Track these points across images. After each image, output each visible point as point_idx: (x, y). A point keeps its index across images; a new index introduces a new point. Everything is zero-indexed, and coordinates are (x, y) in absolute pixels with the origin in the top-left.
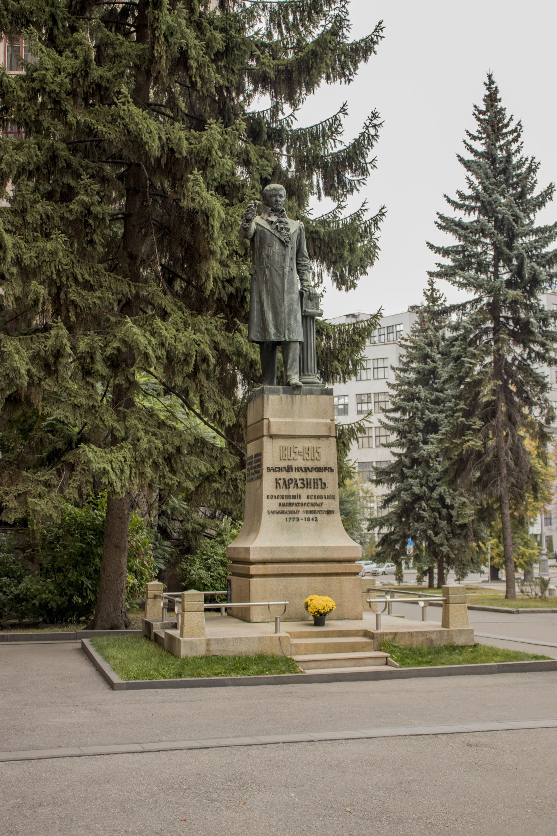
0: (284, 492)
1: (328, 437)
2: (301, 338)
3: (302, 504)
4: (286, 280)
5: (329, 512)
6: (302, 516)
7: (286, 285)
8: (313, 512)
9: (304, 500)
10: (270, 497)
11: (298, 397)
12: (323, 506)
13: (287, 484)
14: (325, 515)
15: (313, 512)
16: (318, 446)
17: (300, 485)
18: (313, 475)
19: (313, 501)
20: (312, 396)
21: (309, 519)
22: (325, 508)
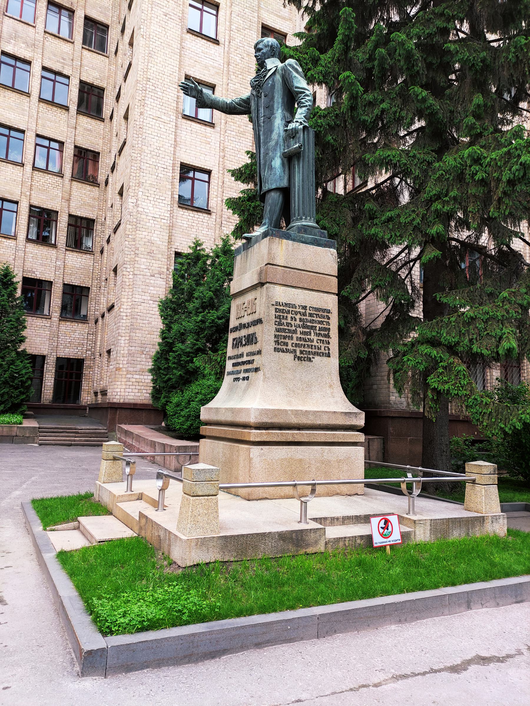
0: (236, 352)
1: (261, 284)
2: (284, 183)
3: (243, 363)
4: (261, 133)
5: (257, 370)
6: (242, 375)
7: (262, 137)
8: (246, 371)
9: (245, 359)
10: (230, 358)
11: (250, 249)
12: (255, 363)
13: (237, 343)
14: (254, 373)
15: (246, 371)
16: (253, 297)
17: (244, 343)
18: (251, 330)
19: (249, 358)
20: (257, 244)
21: (244, 379)
22: (255, 366)
